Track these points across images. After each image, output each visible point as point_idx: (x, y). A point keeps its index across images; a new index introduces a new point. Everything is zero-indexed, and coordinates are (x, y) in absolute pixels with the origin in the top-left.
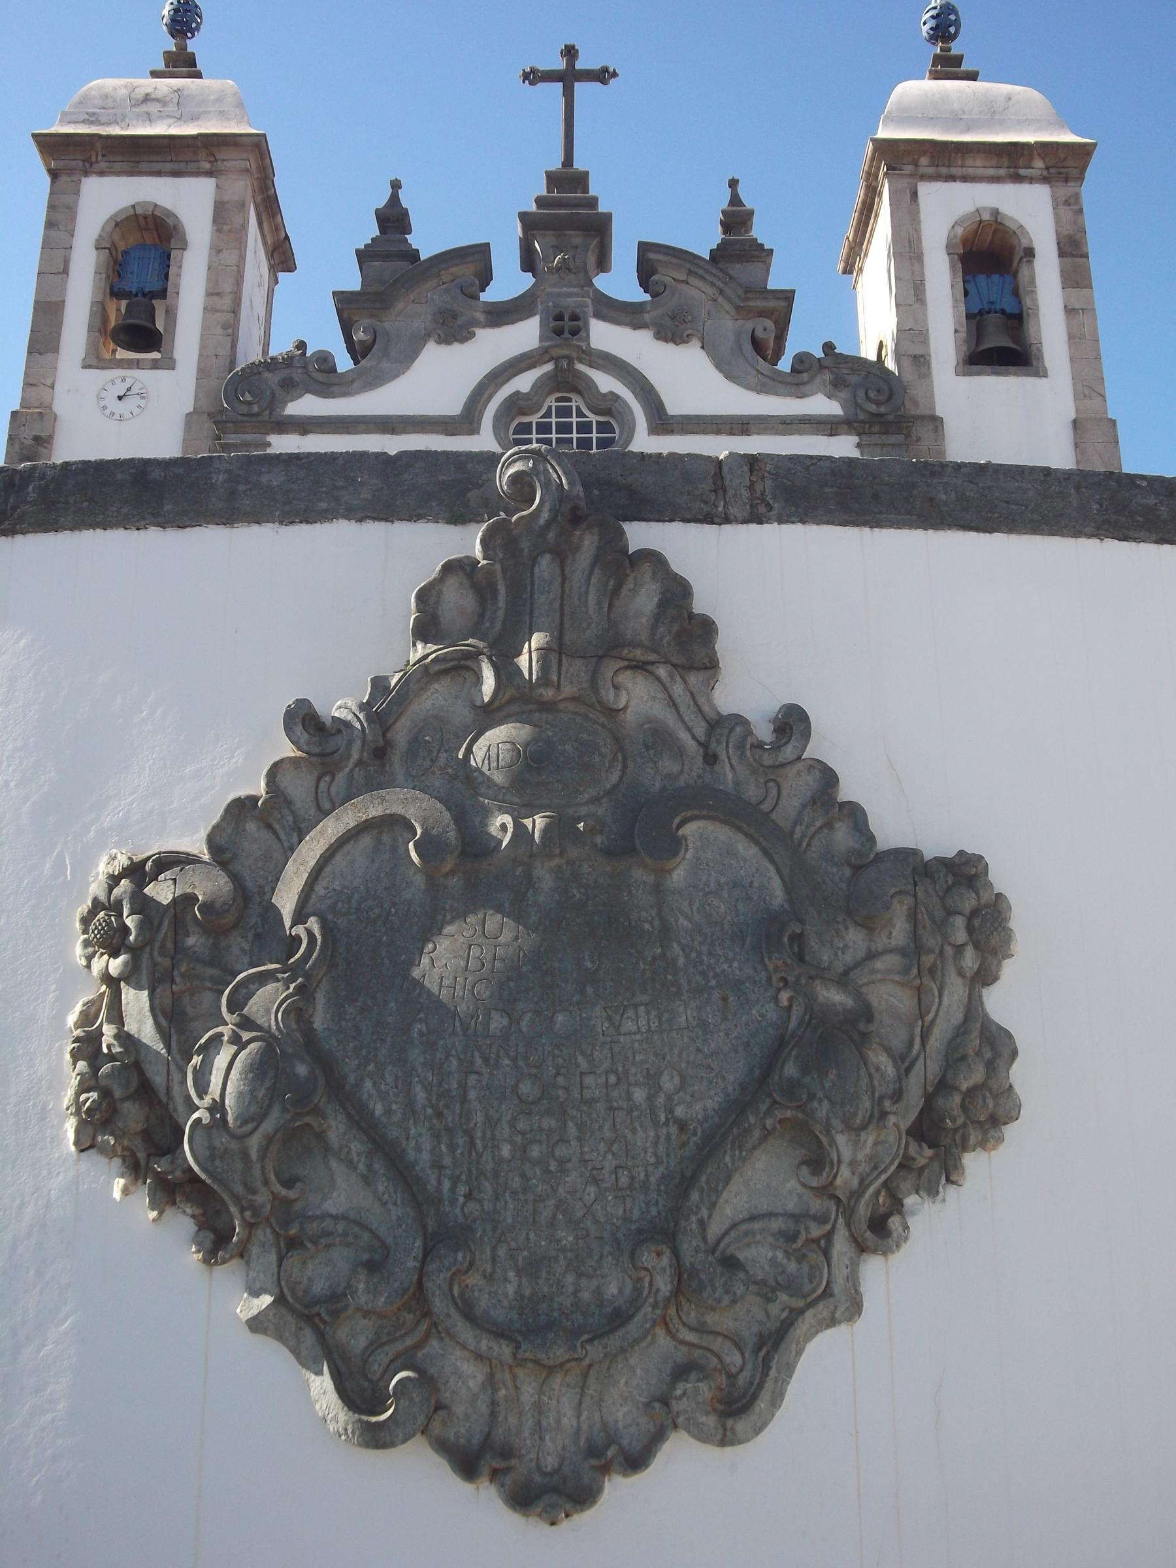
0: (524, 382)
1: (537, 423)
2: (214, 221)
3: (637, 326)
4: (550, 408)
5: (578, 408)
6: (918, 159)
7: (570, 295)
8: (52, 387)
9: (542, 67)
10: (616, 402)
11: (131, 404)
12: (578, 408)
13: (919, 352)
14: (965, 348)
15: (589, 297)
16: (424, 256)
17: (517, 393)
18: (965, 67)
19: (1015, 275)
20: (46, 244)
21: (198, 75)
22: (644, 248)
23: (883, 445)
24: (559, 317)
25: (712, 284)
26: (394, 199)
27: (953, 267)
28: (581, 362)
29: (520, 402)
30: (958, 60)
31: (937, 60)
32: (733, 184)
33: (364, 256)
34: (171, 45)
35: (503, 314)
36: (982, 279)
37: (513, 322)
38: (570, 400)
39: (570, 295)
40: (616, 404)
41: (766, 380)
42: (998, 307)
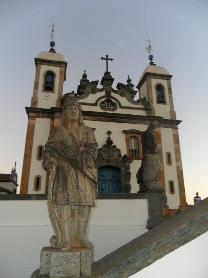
2: (60, 73)
3: (117, 94)
8: (37, 94)
13: (151, 100)
14: (157, 100)
16: (89, 82)
17: (102, 102)
18: (154, 63)
20: (36, 74)
24: (107, 91)
26: (85, 73)
28: (110, 98)
30: (153, 62)
32: (129, 76)
34: (51, 48)
35: (100, 90)
36: (158, 91)
42: (161, 95)
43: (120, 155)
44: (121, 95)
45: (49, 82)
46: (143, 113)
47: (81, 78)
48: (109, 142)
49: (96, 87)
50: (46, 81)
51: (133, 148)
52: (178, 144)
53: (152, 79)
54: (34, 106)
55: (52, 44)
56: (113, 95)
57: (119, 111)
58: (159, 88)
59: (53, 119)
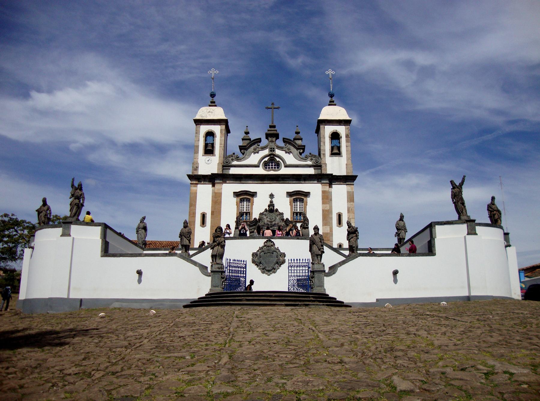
0: (266, 159)
3: (282, 150)
7: (273, 145)
9: (269, 107)
11: (209, 162)
17: (265, 161)
19: (339, 140)
21: (216, 106)
22: (284, 139)
23: (317, 169)
24: (271, 149)
30: (333, 102)
31: (330, 102)
33: (243, 139)
35: (263, 148)
39: (273, 145)
43: (283, 220)
44: (286, 152)
45: (210, 143)
46: (311, 171)
47: (243, 135)
48: (271, 205)
49: (259, 145)
50: (206, 142)
51: (298, 211)
52: (352, 203)
53: (326, 126)
54: (196, 173)
55: (213, 95)
56: (278, 152)
57: (283, 171)
58: (335, 136)
59: (213, 186)
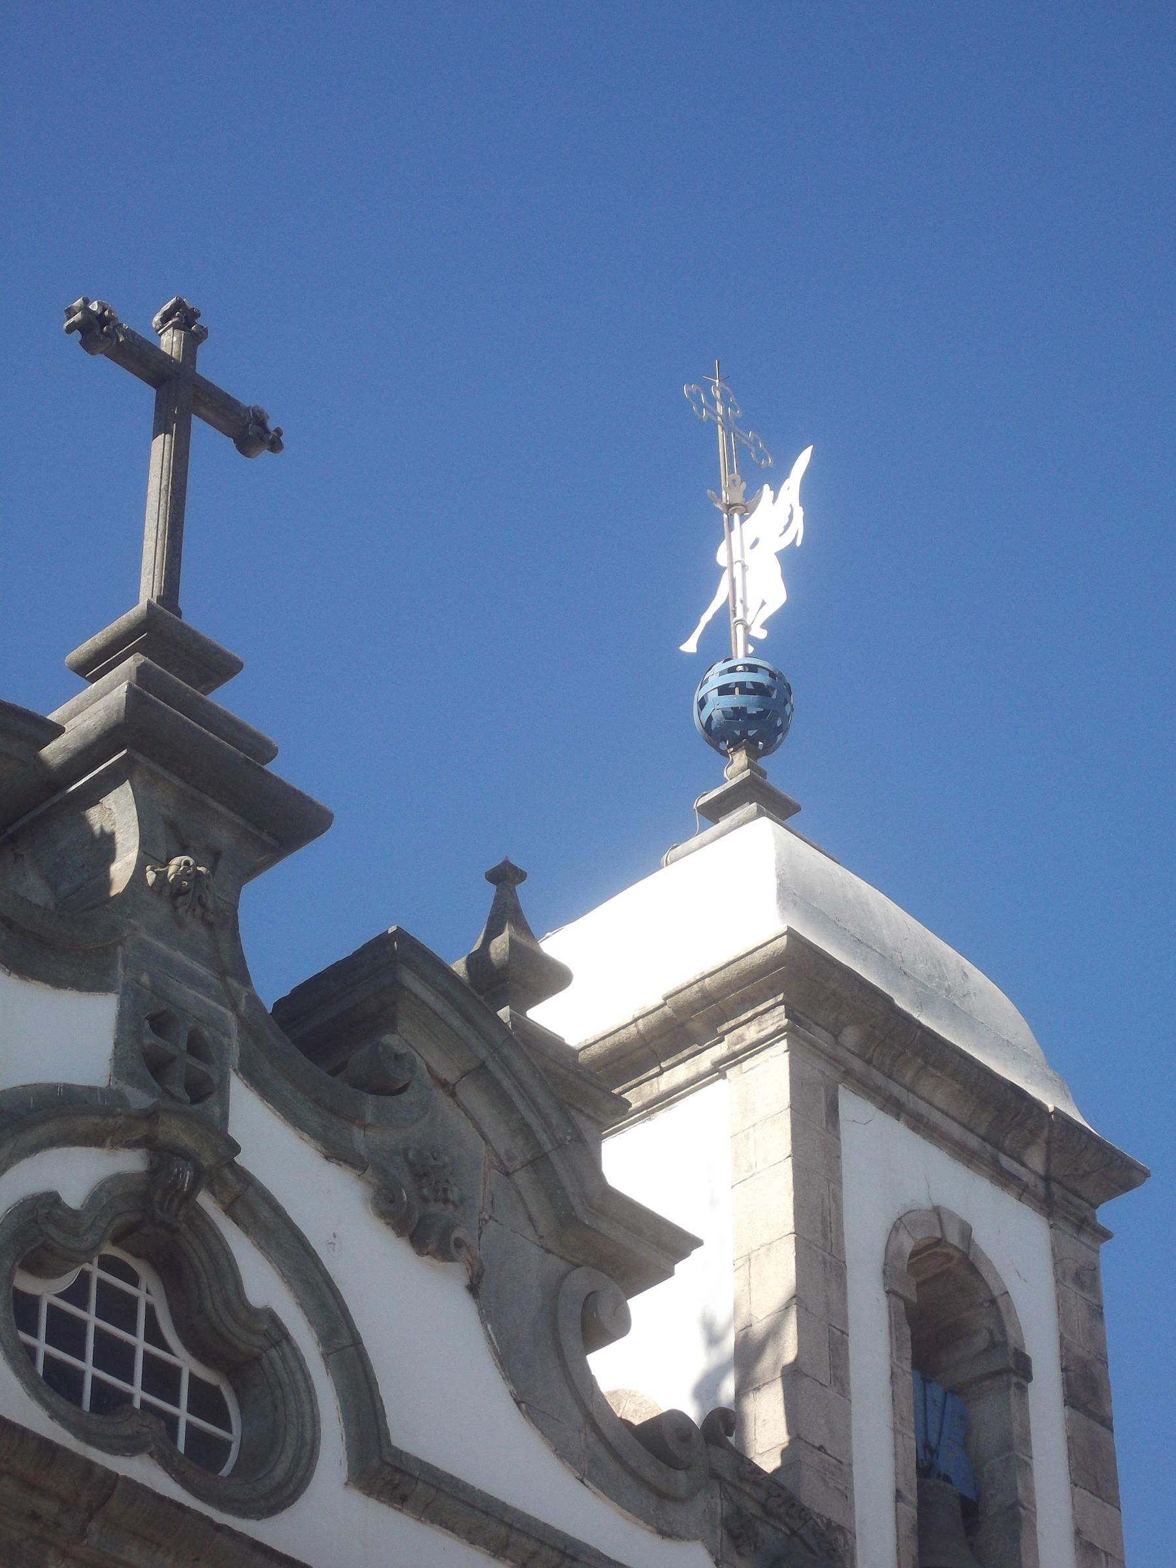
1: (51, 1308)
4: (84, 1277)
5: (150, 1310)
6: (845, 1025)
7: (193, 980)
10: (276, 1344)
12: (150, 1310)
15: (234, 1007)
24: (160, 1023)
25: (525, 1130)
27: (894, 1328)
29: (52, 1230)
37: (58, 983)
38: (133, 1280)
39: (193, 980)
40: (273, 1353)
41: (601, 1452)
